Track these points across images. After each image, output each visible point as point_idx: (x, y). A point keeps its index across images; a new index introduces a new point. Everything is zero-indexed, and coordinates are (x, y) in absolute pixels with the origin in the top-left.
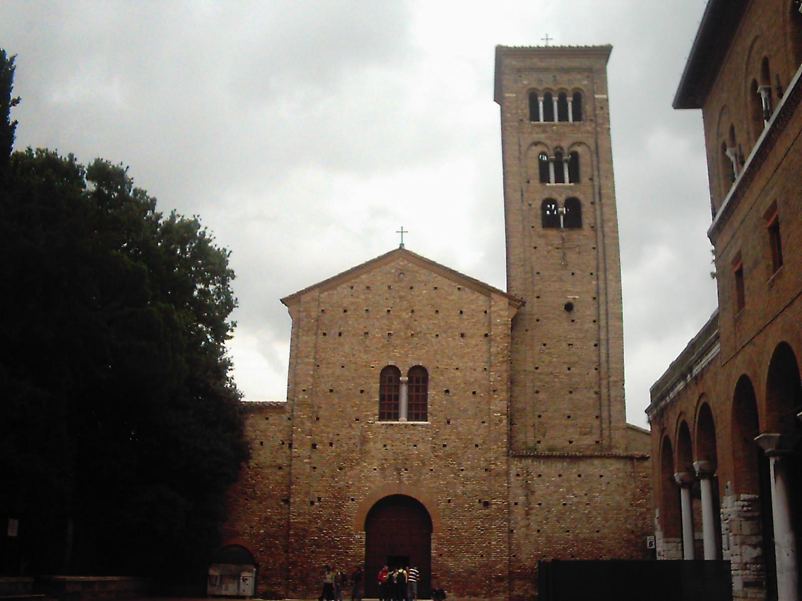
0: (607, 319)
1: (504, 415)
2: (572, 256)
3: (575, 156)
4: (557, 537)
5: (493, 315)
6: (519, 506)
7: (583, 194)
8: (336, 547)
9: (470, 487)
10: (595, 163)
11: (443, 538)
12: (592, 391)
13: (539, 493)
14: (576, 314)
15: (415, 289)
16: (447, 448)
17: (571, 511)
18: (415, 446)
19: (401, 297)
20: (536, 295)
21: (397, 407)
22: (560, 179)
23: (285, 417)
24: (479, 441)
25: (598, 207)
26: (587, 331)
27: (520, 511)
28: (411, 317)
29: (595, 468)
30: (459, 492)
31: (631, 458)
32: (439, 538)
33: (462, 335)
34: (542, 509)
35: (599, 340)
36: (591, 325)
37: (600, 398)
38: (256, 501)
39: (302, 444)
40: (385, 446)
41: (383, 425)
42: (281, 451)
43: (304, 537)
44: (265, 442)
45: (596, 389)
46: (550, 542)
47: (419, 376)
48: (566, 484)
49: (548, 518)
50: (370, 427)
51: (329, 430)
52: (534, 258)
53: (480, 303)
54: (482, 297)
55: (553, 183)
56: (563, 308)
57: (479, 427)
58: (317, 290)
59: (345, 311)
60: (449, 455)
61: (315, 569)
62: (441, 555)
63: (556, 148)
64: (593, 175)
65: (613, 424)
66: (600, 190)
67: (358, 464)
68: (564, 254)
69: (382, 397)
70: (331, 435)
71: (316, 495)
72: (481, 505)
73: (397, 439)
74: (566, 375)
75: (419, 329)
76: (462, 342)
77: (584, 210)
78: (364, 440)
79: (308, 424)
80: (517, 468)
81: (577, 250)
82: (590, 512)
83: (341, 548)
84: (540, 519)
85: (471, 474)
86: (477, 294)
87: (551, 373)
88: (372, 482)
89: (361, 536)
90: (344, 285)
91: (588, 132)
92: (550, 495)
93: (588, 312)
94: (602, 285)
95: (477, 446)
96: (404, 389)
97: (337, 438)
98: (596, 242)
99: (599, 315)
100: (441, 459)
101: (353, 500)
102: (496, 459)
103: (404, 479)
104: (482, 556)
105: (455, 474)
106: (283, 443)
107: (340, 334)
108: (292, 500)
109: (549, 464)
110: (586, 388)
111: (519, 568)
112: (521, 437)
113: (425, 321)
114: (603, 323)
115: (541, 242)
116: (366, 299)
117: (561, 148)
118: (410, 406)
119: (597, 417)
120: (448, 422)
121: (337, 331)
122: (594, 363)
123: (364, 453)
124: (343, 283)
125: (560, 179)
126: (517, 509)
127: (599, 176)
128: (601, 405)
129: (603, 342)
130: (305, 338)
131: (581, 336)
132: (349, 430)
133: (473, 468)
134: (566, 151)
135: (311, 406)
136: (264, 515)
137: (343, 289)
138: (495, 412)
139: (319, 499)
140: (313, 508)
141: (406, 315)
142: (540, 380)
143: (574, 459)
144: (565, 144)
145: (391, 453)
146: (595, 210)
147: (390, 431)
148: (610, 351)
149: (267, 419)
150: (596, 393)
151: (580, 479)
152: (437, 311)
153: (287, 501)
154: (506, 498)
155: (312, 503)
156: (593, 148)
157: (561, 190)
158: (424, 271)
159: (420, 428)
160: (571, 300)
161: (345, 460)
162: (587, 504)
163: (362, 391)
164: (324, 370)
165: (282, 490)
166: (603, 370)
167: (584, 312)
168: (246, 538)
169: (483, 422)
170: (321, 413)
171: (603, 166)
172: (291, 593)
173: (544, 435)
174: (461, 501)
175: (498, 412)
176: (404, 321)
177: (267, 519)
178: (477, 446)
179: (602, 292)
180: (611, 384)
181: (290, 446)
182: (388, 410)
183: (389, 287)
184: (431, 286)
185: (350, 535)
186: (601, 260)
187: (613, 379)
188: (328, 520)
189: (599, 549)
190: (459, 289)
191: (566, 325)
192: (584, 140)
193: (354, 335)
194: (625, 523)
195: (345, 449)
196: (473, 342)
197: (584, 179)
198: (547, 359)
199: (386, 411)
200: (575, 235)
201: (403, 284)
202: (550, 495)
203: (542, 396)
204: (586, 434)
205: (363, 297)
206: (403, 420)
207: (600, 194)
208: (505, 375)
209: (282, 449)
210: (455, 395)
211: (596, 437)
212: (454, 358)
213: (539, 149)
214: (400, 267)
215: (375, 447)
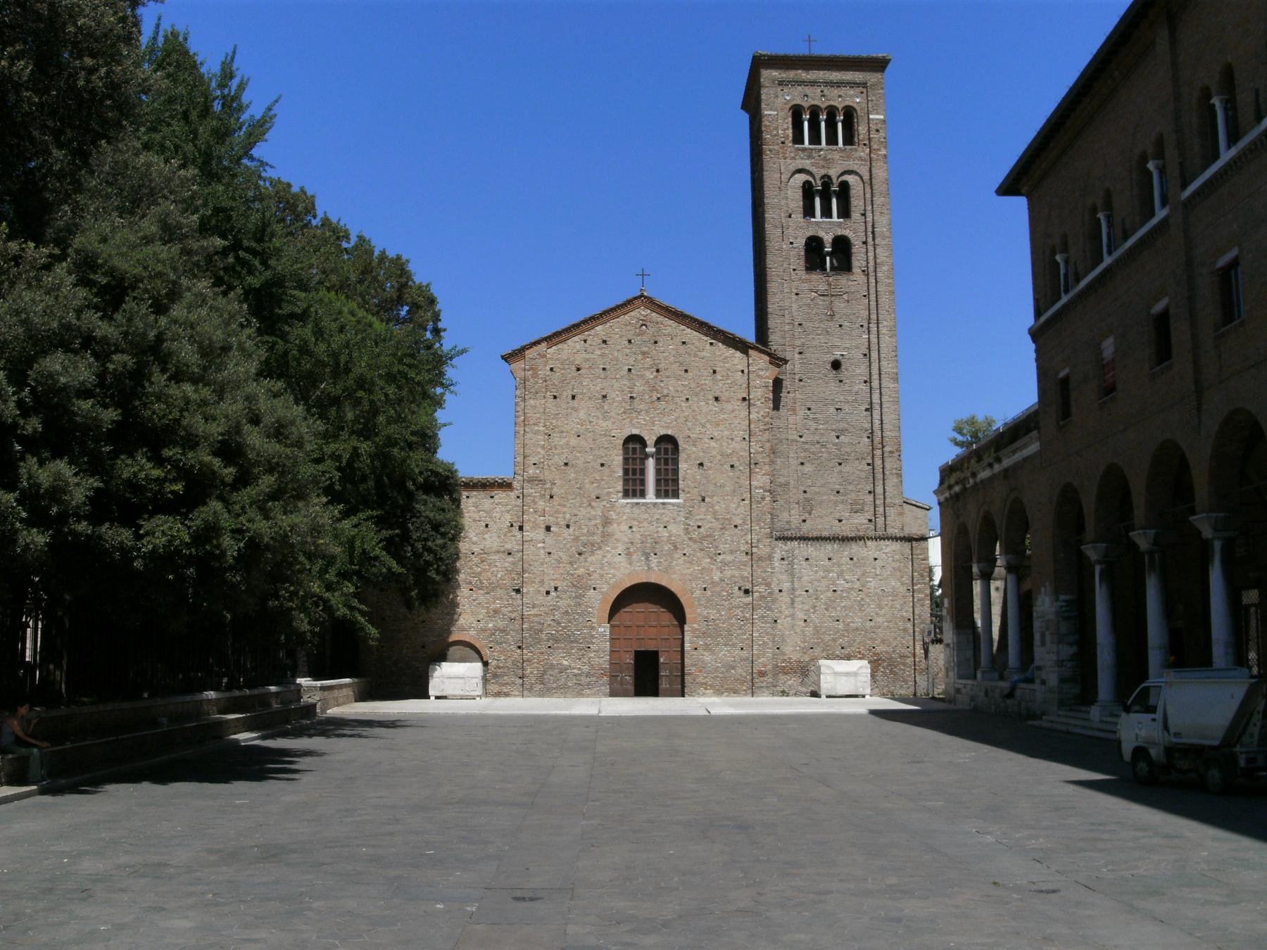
1: (765, 491)
2: (839, 305)
3: (845, 186)
6: (783, 594)
7: (853, 230)
9: (728, 573)
10: (868, 196)
12: (864, 462)
13: (806, 578)
14: (844, 373)
15: (660, 344)
19: (644, 353)
20: (797, 350)
21: (643, 482)
22: (827, 212)
23: (513, 494)
24: (739, 522)
25: (871, 248)
26: (857, 393)
27: (785, 598)
29: (870, 550)
30: (716, 578)
31: (909, 539)
32: (694, 630)
33: (717, 399)
35: (871, 403)
36: (863, 386)
39: (535, 526)
43: (541, 631)
44: (491, 524)
48: (836, 569)
50: (613, 506)
52: (795, 307)
53: (736, 361)
54: (738, 354)
55: (818, 218)
56: (829, 366)
57: (739, 505)
58: (544, 344)
59: (578, 369)
60: (703, 538)
61: (552, 667)
63: (823, 177)
65: (888, 500)
67: (600, 548)
69: (626, 471)
70: (568, 516)
71: (553, 584)
72: (741, 593)
75: (665, 392)
76: (715, 407)
77: (854, 250)
78: (607, 522)
79: (541, 504)
81: (845, 297)
84: (807, 607)
85: (729, 558)
86: (732, 351)
89: (605, 629)
90: (576, 338)
91: (861, 159)
92: (819, 581)
94: (874, 340)
97: (574, 519)
100: (695, 542)
102: (758, 541)
107: (573, 397)
112: (784, 516)
113: (672, 381)
114: (875, 384)
115: (806, 286)
116: (603, 355)
117: (829, 177)
118: (658, 482)
121: (570, 393)
123: (606, 536)
125: (827, 212)
129: (876, 407)
130: (532, 402)
132: (589, 509)
133: (732, 552)
134: (834, 180)
135: (542, 482)
136: (493, 606)
137: (575, 343)
139: (556, 589)
140: (549, 598)
141: (650, 375)
142: (805, 451)
143: (845, 539)
144: (833, 173)
145: (638, 536)
147: (636, 510)
154: (768, 585)
155: (548, 593)
156: (866, 177)
159: (670, 507)
160: (838, 357)
161: (584, 545)
163: (602, 465)
164: (556, 439)
166: (877, 439)
167: (856, 370)
168: (473, 633)
170: (555, 490)
172: (526, 693)
174: (718, 589)
176: (647, 382)
177: (496, 611)
179: (874, 347)
181: (521, 528)
183: (630, 341)
184: (678, 340)
185: (593, 628)
186: (873, 311)
187: (887, 449)
189: (873, 639)
191: (833, 385)
192: (855, 168)
193: (590, 398)
196: (729, 407)
197: (856, 215)
198: (813, 425)
199: (630, 488)
200: (843, 281)
201: (645, 338)
202: (819, 581)
203: (808, 468)
205: (599, 352)
207: (873, 232)
208: (768, 445)
210: (710, 468)
211: (869, 515)
212: (708, 426)
213: (802, 178)
215: (620, 530)
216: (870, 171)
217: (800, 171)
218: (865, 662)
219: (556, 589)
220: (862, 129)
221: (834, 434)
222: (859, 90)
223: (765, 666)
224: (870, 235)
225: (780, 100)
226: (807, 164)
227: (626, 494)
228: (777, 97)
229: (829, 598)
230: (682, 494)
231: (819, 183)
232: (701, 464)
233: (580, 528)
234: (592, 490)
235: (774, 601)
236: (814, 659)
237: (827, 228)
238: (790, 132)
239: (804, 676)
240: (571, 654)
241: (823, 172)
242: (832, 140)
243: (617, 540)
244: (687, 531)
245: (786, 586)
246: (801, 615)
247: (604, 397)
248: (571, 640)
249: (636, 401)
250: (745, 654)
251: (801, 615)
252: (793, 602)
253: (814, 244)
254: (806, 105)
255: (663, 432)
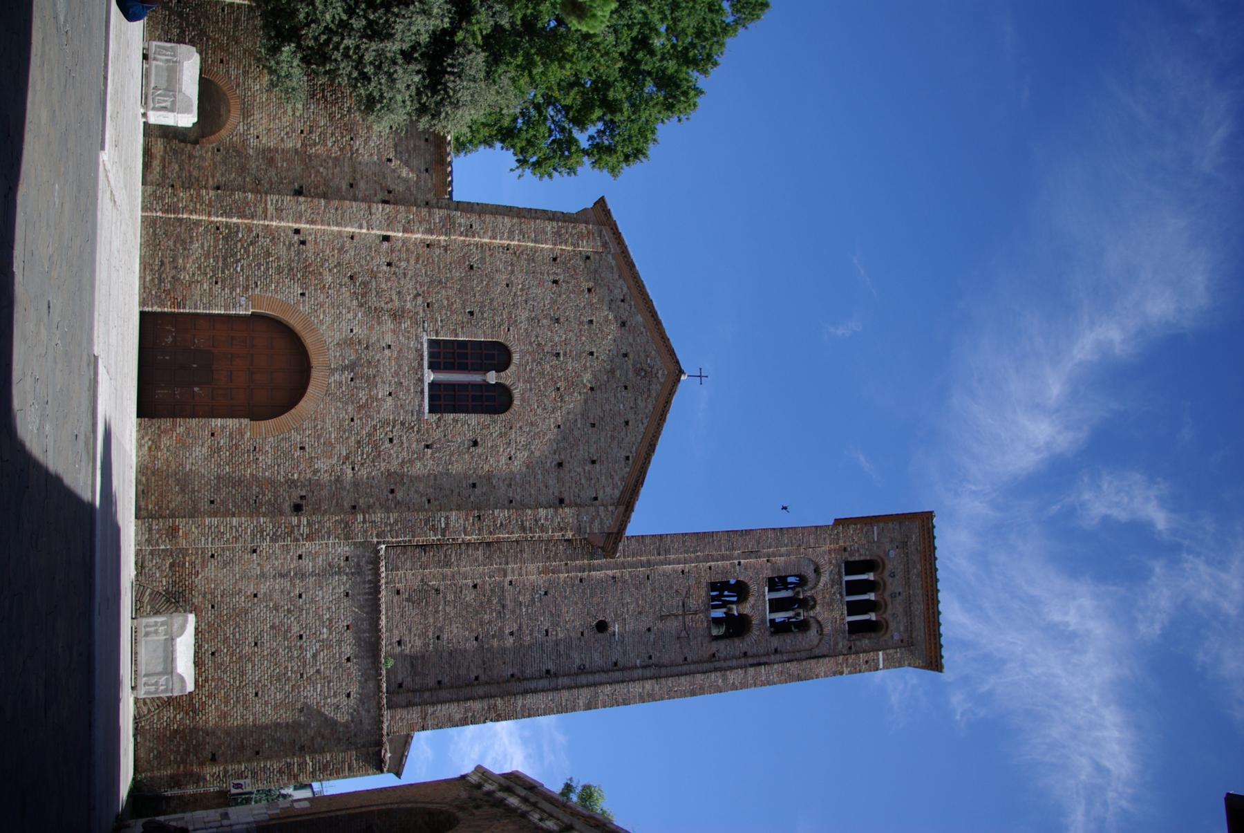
0: (588, 686)
3: (803, 626)
4: (246, 627)
5: (592, 509)
8: (226, 266)
10: (798, 655)
11: (242, 436)
12: (480, 672)
16: (387, 445)
17: (290, 649)
18: (390, 394)
19: (612, 371)
22: (776, 605)
24: (399, 495)
26: (568, 657)
28: (585, 386)
30: (318, 465)
33: (560, 465)
34: (291, 600)
35: (556, 675)
36: (578, 662)
37: (470, 685)
38: (299, 145)
40: (389, 347)
41: (422, 344)
42: (378, 188)
45: (482, 677)
46: (238, 615)
47: (496, 401)
49: (277, 610)
51: (412, 262)
53: (608, 490)
54: (617, 493)
60: (376, 446)
62: (213, 435)
64: (781, 653)
66: (765, 664)
67: (361, 305)
68: (676, 616)
73: (400, 366)
74: (501, 629)
78: (396, 316)
80: (358, 556)
82: (288, 679)
83: (223, 272)
84: (276, 596)
87: (504, 606)
88: (328, 326)
90: (625, 290)
91: (836, 644)
93: (596, 656)
94: (636, 673)
95: (392, 491)
96: (475, 378)
98: (694, 663)
99: (593, 673)
101: (303, 294)
103: (337, 376)
104: (212, 502)
105: (347, 458)
106: (390, 192)
107: (555, 282)
108: (301, 199)
109: (366, 610)
110: (484, 663)
111: (192, 564)
114: (583, 679)
115: (692, 582)
117: (813, 607)
119: (439, 682)
120: (427, 447)
122: (522, 672)
124: (629, 288)
126: (292, 559)
127: (782, 662)
128: (459, 687)
131: (562, 647)
138: (447, 518)
139: (303, 243)
142: (492, 591)
144: (818, 608)
146: (734, 657)
148: (540, 696)
149: (427, 170)
150: (477, 678)
151: (344, 661)
152: (593, 425)
153: (299, 192)
154: (309, 537)
156: (817, 652)
157: (757, 607)
158: (650, 407)
160: (611, 629)
162: (302, 675)
165: (316, 188)
169: (429, 501)
171: (793, 667)
173: (408, 600)
175: (447, 524)
178: (392, 491)
179: (626, 674)
180: (492, 701)
181: (385, 202)
182: (446, 355)
183: (625, 355)
184: (630, 416)
185: (246, 289)
188: (268, 254)
190: (627, 458)
192: (826, 638)
194: (273, 740)
195: (383, 286)
197: (776, 642)
201: (631, 374)
203: (470, 596)
204: (412, 665)
206: (429, 376)
207: (759, 664)
209: (382, 188)
214: (654, 371)
215: (386, 331)
216: (824, 656)
217: (817, 571)
218: (190, 687)
219: (303, 243)
220: (865, 642)
221: (515, 627)
222: (905, 636)
223: (186, 535)
224: (755, 661)
225: (888, 547)
226: (825, 578)
227: (432, 343)
228: (892, 541)
229: (289, 629)
230: (435, 417)
231: (809, 594)
232: (475, 443)
233: (388, 280)
234: (440, 297)
235: (286, 549)
236: (196, 610)
237: (757, 607)
238: (856, 558)
239: (170, 597)
240: (207, 256)
241: (819, 598)
242: (853, 608)
243: (371, 328)
244: (385, 423)
245: (308, 564)
246: (263, 589)
247: (557, 320)
248: (228, 258)
249: (555, 362)
250: (204, 506)
251: (263, 589)
252: (282, 576)
253: (741, 590)
254: (886, 573)
255: (516, 394)
